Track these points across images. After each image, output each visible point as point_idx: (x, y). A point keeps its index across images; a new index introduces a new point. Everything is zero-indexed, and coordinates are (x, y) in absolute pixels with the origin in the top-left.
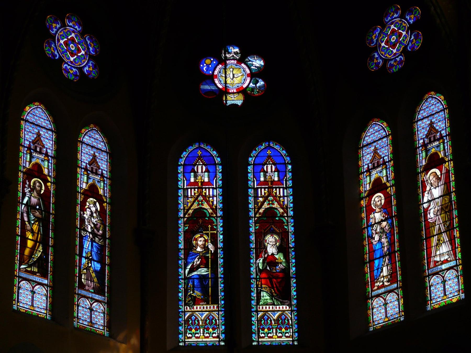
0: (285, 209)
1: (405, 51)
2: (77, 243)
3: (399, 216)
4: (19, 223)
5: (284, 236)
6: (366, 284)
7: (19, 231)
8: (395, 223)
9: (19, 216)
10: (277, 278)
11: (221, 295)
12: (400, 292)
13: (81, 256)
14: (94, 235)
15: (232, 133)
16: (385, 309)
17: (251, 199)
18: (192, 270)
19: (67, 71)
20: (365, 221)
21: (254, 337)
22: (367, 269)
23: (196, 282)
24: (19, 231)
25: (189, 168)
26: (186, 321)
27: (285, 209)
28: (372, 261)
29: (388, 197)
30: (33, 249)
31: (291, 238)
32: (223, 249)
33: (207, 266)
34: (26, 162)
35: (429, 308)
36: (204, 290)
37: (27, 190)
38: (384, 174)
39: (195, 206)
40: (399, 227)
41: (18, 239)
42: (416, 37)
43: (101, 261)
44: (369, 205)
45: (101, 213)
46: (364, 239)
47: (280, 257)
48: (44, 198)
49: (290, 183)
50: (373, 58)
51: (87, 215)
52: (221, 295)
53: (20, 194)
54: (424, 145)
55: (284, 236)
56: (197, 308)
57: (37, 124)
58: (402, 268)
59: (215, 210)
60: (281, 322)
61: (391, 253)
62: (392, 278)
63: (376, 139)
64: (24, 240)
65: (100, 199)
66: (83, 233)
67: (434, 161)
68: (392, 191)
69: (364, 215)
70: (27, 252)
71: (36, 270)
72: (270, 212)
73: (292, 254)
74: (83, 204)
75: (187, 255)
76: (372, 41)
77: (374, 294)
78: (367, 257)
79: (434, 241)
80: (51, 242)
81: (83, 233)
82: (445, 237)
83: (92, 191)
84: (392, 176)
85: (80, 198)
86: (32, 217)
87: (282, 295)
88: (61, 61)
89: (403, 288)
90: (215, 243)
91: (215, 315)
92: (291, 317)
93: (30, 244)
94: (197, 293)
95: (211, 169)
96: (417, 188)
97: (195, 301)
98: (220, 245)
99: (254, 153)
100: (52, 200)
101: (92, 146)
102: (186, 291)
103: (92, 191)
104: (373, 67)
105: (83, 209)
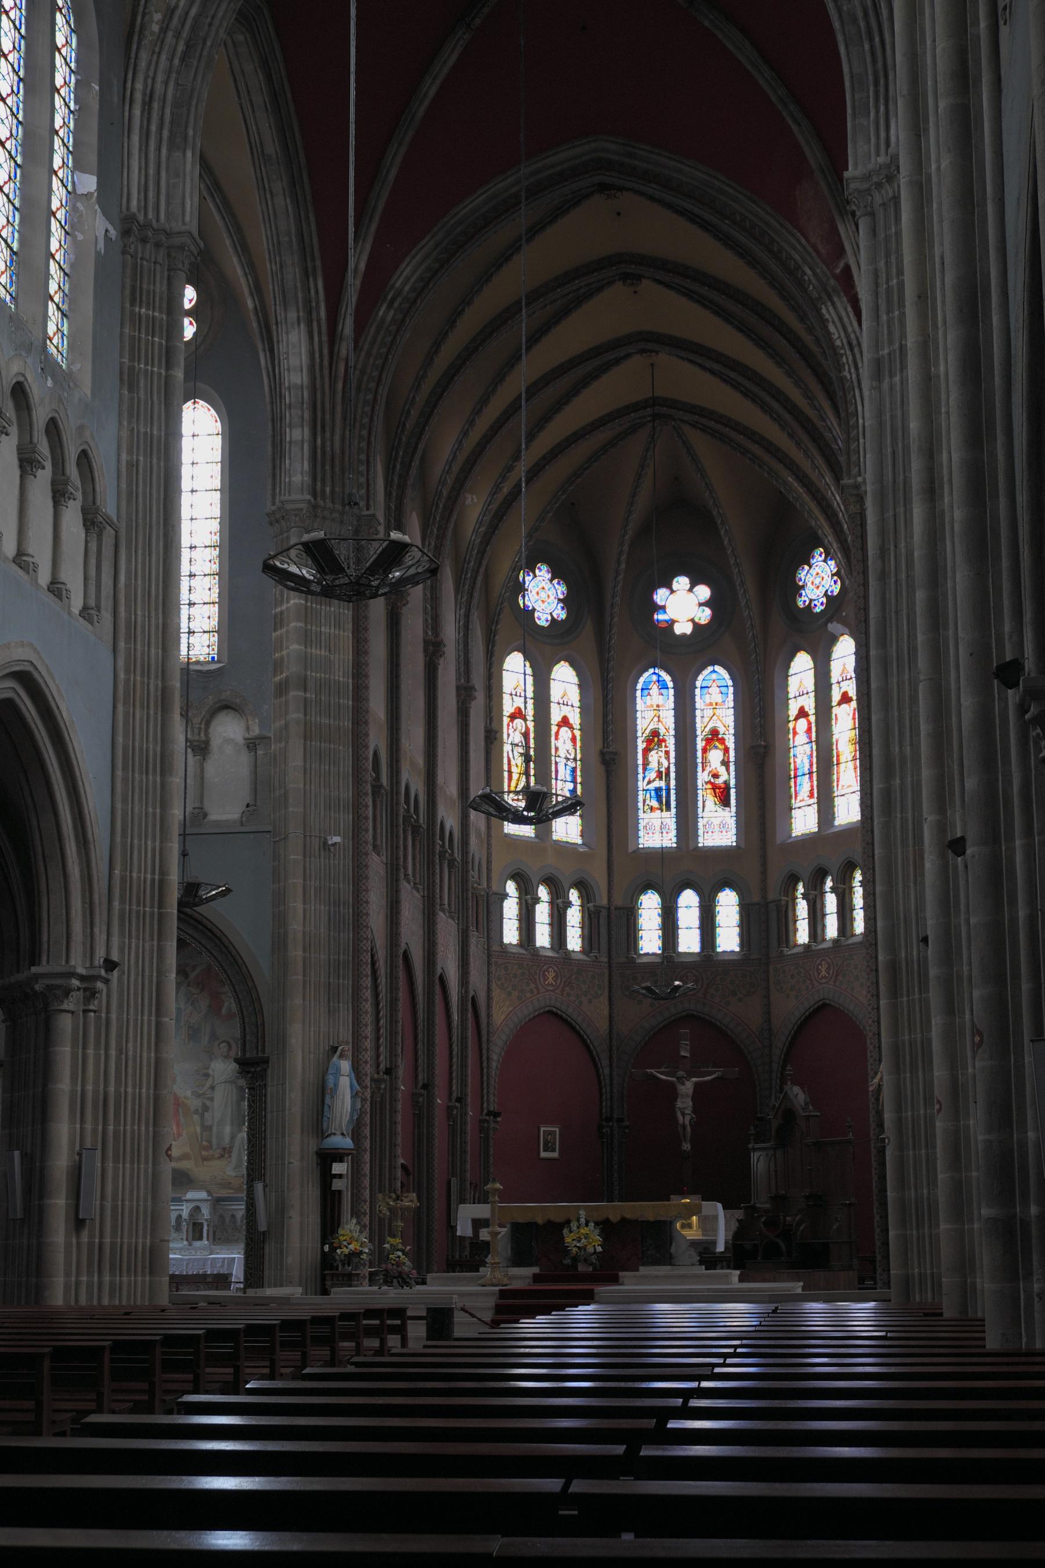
0: (726, 727)
1: (826, 594)
2: (553, 768)
3: (817, 742)
4: (505, 761)
5: (726, 750)
6: (791, 797)
7: (506, 767)
8: (814, 747)
9: (505, 755)
10: (720, 788)
11: (673, 804)
12: (816, 806)
13: (556, 779)
14: (568, 759)
15: (684, 657)
16: (804, 821)
17: (698, 720)
18: (649, 782)
19: (539, 619)
20: (791, 742)
21: (700, 839)
22: (792, 784)
23: (653, 793)
24: (506, 767)
25: (646, 692)
26: (645, 827)
27: (726, 727)
28: (796, 777)
29: (809, 723)
30: (518, 780)
31: (732, 753)
32: (676, 764)
33: (661, 779)
34: (508, 707)
35: (837, 823)
36: (659, 798)
37: (511, 731)
38: (809, 703)
39: (651, 727)
40: (817, 750)
41: (506, 774)
42: (835, 582)
43: (574, 781)
44: (794, 729)
45: (574, 739)
46: (789, 758)
47: (722, 770)
48: (526, 735)
49: (732, 704)
50: (801, 595)
51: (560, 744)
52: (673, 804)
53: (505, 736)
54: (838, 683)
55: (726, 750)
56: (653, 815)
57: (515, 671)
58: (818, 786)
59: (667, 730)
60: (723, 825)
61: (811, 773)
62: (811, 796)
63: (802, 665)
64: (510, 772)
65: (571, 727)
66: (558, 759)
67: (845, 699)
68: (812, 718)
69: (791, 736)
70: (513, 784)
71: (521, 797)
72: (715, 732)
73: (732, 768)
74: (557, 734)
75: (645, 770)
76: (800, 580)
77: (797, 805)
78: (792, 773)
79: (842, 766)
80: (532, 772)
81: (558, 759)
82: (851, 765)
83: (565, 722)
84: (813, 705)
85: (554, 729)
86: (515, 753)
87: (725, 802)
88: (534, 610)
89: (818, 803)
90: (668, 758)
91: (668, 821)
92: (732, 822)
93: (515, 776)
94: (655, 804)
95: (664, 691)
96: (830, 719)
97: (652, 809)
98: (672, 760)
99: (701, 677)
100: (532, 735)
101: (564, 680)
102: (644, 801)
103: (565, 722)
104: (801, 604)
105: (557, 738)
